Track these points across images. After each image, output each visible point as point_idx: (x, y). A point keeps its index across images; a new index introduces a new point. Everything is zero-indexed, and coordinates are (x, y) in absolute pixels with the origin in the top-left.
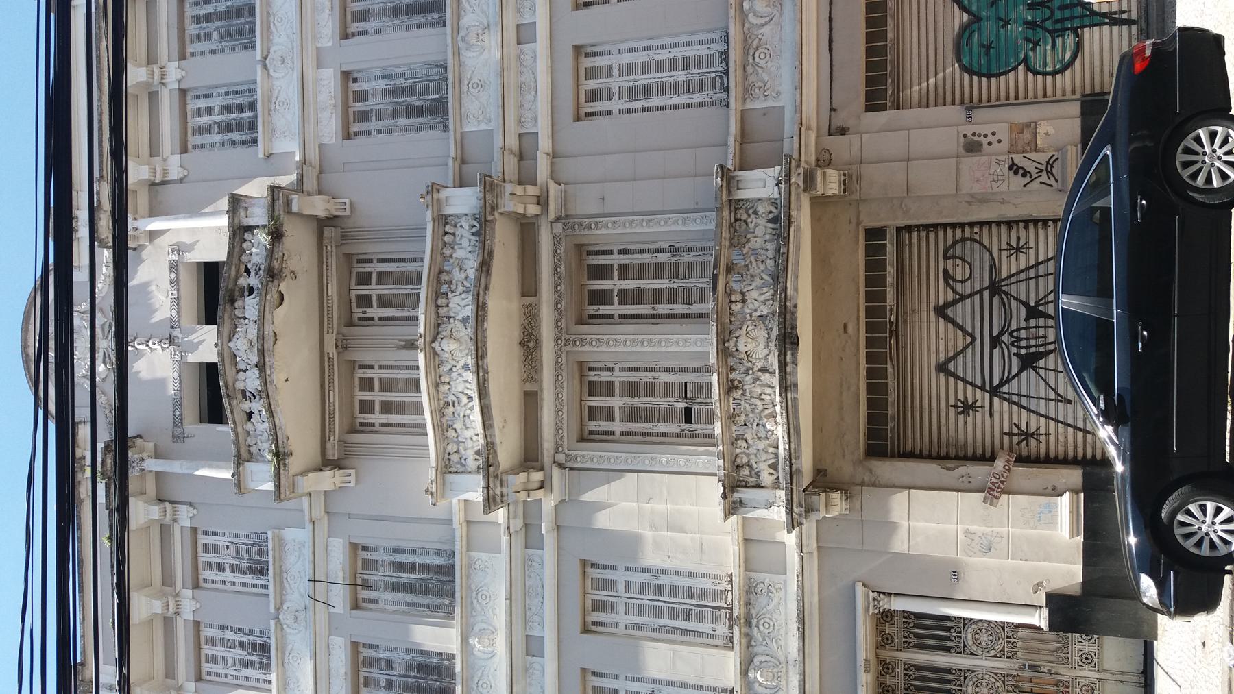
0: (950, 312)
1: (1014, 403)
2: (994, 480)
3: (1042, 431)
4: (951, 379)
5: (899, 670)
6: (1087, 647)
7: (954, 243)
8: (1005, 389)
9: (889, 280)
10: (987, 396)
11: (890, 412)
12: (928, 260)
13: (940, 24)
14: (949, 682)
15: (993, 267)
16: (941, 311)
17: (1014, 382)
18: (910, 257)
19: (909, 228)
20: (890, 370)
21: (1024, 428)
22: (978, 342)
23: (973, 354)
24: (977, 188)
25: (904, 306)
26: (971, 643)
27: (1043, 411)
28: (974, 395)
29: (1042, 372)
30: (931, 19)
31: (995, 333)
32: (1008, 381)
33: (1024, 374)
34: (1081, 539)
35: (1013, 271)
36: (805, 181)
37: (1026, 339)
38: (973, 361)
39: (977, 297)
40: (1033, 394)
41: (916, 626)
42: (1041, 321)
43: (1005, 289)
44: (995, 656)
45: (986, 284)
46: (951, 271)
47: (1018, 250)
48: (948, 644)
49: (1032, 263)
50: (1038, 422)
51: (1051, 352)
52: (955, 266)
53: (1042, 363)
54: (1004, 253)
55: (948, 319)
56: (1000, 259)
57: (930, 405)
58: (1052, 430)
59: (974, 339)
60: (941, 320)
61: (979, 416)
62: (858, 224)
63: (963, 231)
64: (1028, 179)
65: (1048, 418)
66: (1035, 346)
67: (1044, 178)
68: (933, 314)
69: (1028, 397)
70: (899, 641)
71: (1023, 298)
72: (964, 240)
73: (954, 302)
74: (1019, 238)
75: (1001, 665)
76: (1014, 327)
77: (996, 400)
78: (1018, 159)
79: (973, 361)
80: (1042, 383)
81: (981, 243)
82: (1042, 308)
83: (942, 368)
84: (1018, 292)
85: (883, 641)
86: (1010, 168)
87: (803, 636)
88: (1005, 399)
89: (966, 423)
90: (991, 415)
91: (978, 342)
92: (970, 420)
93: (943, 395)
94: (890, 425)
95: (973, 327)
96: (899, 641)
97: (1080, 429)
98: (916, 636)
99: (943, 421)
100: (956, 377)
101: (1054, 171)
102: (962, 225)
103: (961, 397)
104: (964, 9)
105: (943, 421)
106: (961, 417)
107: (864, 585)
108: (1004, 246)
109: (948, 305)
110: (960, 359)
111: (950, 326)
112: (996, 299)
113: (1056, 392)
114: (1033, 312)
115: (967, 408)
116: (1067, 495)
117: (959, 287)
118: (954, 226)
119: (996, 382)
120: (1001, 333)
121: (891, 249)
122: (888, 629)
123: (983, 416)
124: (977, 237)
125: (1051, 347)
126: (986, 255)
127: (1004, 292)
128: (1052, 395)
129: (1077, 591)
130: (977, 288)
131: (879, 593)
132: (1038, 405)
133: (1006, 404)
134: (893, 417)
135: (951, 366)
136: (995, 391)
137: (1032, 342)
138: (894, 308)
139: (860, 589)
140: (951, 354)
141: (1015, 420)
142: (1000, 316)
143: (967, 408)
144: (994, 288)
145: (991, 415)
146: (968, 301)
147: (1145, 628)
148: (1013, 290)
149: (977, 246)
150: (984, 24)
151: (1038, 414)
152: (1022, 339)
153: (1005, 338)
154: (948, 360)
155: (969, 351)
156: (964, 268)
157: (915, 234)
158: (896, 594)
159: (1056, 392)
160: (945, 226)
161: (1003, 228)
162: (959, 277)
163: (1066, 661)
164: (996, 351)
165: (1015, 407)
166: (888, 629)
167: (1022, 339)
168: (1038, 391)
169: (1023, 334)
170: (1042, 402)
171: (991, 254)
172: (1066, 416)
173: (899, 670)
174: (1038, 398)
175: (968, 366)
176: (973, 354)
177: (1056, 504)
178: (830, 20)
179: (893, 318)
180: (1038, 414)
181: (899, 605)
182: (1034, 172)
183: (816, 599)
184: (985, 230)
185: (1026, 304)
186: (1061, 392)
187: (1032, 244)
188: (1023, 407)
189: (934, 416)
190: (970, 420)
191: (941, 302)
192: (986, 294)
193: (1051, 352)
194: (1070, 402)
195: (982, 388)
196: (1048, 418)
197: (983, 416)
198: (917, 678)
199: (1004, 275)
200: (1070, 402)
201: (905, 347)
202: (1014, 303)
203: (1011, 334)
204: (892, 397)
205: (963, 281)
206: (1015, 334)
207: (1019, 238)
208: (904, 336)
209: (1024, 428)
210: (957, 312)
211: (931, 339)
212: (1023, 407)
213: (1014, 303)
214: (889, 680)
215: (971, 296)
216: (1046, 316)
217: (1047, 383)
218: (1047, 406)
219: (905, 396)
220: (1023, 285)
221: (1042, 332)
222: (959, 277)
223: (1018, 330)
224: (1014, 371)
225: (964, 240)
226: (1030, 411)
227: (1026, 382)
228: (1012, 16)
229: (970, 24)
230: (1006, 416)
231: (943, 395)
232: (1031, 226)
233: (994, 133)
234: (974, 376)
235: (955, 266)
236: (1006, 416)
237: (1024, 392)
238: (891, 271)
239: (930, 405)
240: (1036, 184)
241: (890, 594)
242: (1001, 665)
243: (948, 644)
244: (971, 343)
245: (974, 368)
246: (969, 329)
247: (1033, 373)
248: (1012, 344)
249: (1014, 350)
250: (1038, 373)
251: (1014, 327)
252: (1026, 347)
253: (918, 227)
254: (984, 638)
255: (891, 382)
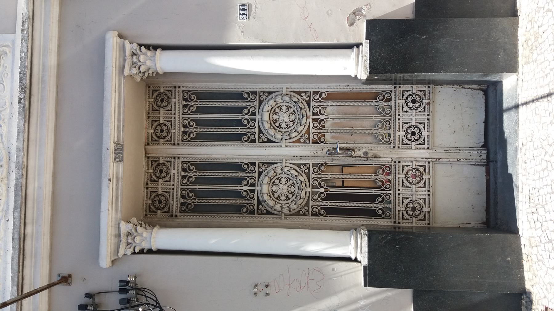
5: (176, 172)
6: (414, 118)
14: (238, 181)
26: (267, 126)
41: (200, 110)
44: (298, 141)
48: (240, 130)
70: (176, 131)
75: (305, 152)
85: (159, 133)
87: (27, 113)
96: (176, 131)
98: (199, 123)
107: (121, 36)
122: (162, 116)
129: (409, 14)
131: (140, 45)
139: (112, 39)
147: (502, 56)
158: (166, 48)
163: (388, 140)
166: (162, 116)
173: (176, 172)
181: (167, 62)
183: (52, 60)
198: (198, 180)
214: (161, 186)
241: (155, 48)
242: (305, 152)
243: (240, 130)
254: (284, 118)
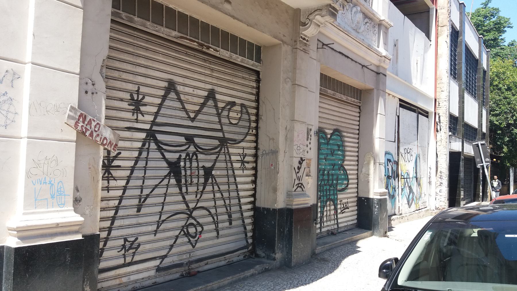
0: (211, 103)
1: (140, 154)
2: (94, 124)
3: (112, 183)
4: (162, 93)
7: (248, 114)
8: (153, 146)
9: (234, 56)
10: (147, 127)
11: (136, 19)
12: (233, 90)
13: (328, 122)
15: (236, 142)
16: (211, 95)
17: (158, 155)
18: (243, 78)
19: (258, 81)
20: (175, 33)
21: (116, 163)
22: (190, 123)
23: (182, 118)
24: (296, 134)
25: (215, 64)
27: (132, 183)
28: (148, 113)
29: (166, 182)
30: (344, 116)
31: (196, 140)
32: (160, 149)
33: (165, 164)
34: (13, 242)
35: (233, 158)
36: (334, 8)
37: (190, 167)
38: (175, 117)
39: (219, 127)
40: (149, 173)
42: (202, 180)
43: (223, 151)
45: (227, 136)
46: (235, 108)
47: (243, 162)
49: (237, 172)
50: (121, 178)
51: (181, 189)
52: (236, 111)
53: (173, 181)
54: (240, 151)
55: (207, 98)
56: (238, 148)
57: (139, 65)
58: (112, 193)
59: (193, 120)
60: (206, 94)
61: (129, 115)
62: (284, 42)
63: (254, 122)
64: (297, 171)
65: (125, 189)
66: (185, 176)
67: (297, 182)
68: (209, 87)
69: (145, 169)
71: (218, 165)
72: (249, 121)
73: (216, 107)
74: (248, 162)
76: (200, 156)
77: (143, 135)
78: (304, 163)
79: (175, 117)
80: (157, 182)
81: (247, 134)
82: (210, 181)
83: (171, 87)
84: (221, 161)
86: (301, 158)
88: (144, 145)
89: (122, 100)
90: (129, 129)
91: (190, 123)
92: (125, 105)
93: (149, 81)
94: (124, 15)
95: (201, 121)
97: (112, 223)
99: (124, 76)
100: (164, 98)
101: (299, 188)
102: (257, 121)
103: (147, 99)
104: (332, 135)
105: (124, 76)
106: (127, 96)
108: (247, 151)
109: (215, 100)
110: (178, 105)
111: (202, 101)
112: (216, 142)
113: (148, 196)
114: (208, 172)
115: (137, 104)
116: (78, 218)
117: (225, 113)
118: (257, 115)
119: (160, 137)
120: (196, 146)
121: (250, 63)
123: (128, 120)
124: (250, 132)
125: (184, 190)
126: (241, 137)
127: (221, 150)
128: (146, 192)
130: (225, 128)
132: (138, 178)
133: (139, 145)
134: (131, 21)
135: (172, 95)
136: (151, 135)
137: (188, 173)
138: (217, 54)
140: (182, 97)
141: (124, 154)
142: (207, 145)
143: (137, 104)
144: (224, 142)
145: (129, 129)
146: (216, 119)
148: (222, 157)
149: (246, 131)
150: (326, 146)
151: (129, 179)
152: (191, 163)
153: (192, 149)
154: (177, 93)
155: (183, 114)
156: (235, 119)
157: (254, 85)
159: (148, 196)
160: (257, 108)
161: (253, 152)
162: (232, 114)
164: (182, 140)
165: (136, 154)
167: (191, 163)
168: (150, 178)
169: (195, 164)
170: (139, 183)
171: (242, 140)
172: (126, 207)
174: (144, 178)
175: (172, 113)
176: (182, 118)
177: (64, 204)
178: (348, 57)
179: (211, 51)
180: (129, 179)
182: (298, 175)
184: (253, 138)
185: (212, 168)
186: (149, 201)
187: (246, 172)
188: (136, 163)
189: (129, 67)
190: (125, 105)
191: (218, 96)
192: (220, 135)
193: (181, 189)
194: (139, 210)
195: (153, 123)
196: (125, 189)
197: (128, 120)
199: (231, 150)
200: (139, 210)
201: (187, 54)
202: (214, 157)
203: (194, 154)
204: (150, 27)
205: (228, 117)
206: (195, 157)
207: (248, 162)
208: (195, 57)
209: (116, 163)
210: (209, 109)
211: (196, 81)
212: (136, 163)
213: (214, 157)
215: (220, 122)
216: (205, 185)
217: (156, 186)
218: (136, 187)
219: (147, 41)
220: (223, 165)
221: (195, 181)
222: (232, 114)
223: (197, 160)
224: (168, 155)
225: (249, 121)
226: (133, 169)
227: (158, 167)
228: (327, 162)
229: (326, 138)
230: (127, 144)
231: (149, 81)
232: (253, 172)
233: (310, 149)
234: (164, 116)
235: (236, 111)
236: (127, 144)
237: (150, 164)
238: (238, 59)
239: (139, 65)
240: (294, 176)
244: (189, 117)
245: (171, 116)
246: (200, 117)
247: (166, 172)
248: (188, 154)
249: (184, 155)
250: (165, 177)
251: (200, 156)
252: (184, 167)
253: (258, 88)
255: (164, 31)
